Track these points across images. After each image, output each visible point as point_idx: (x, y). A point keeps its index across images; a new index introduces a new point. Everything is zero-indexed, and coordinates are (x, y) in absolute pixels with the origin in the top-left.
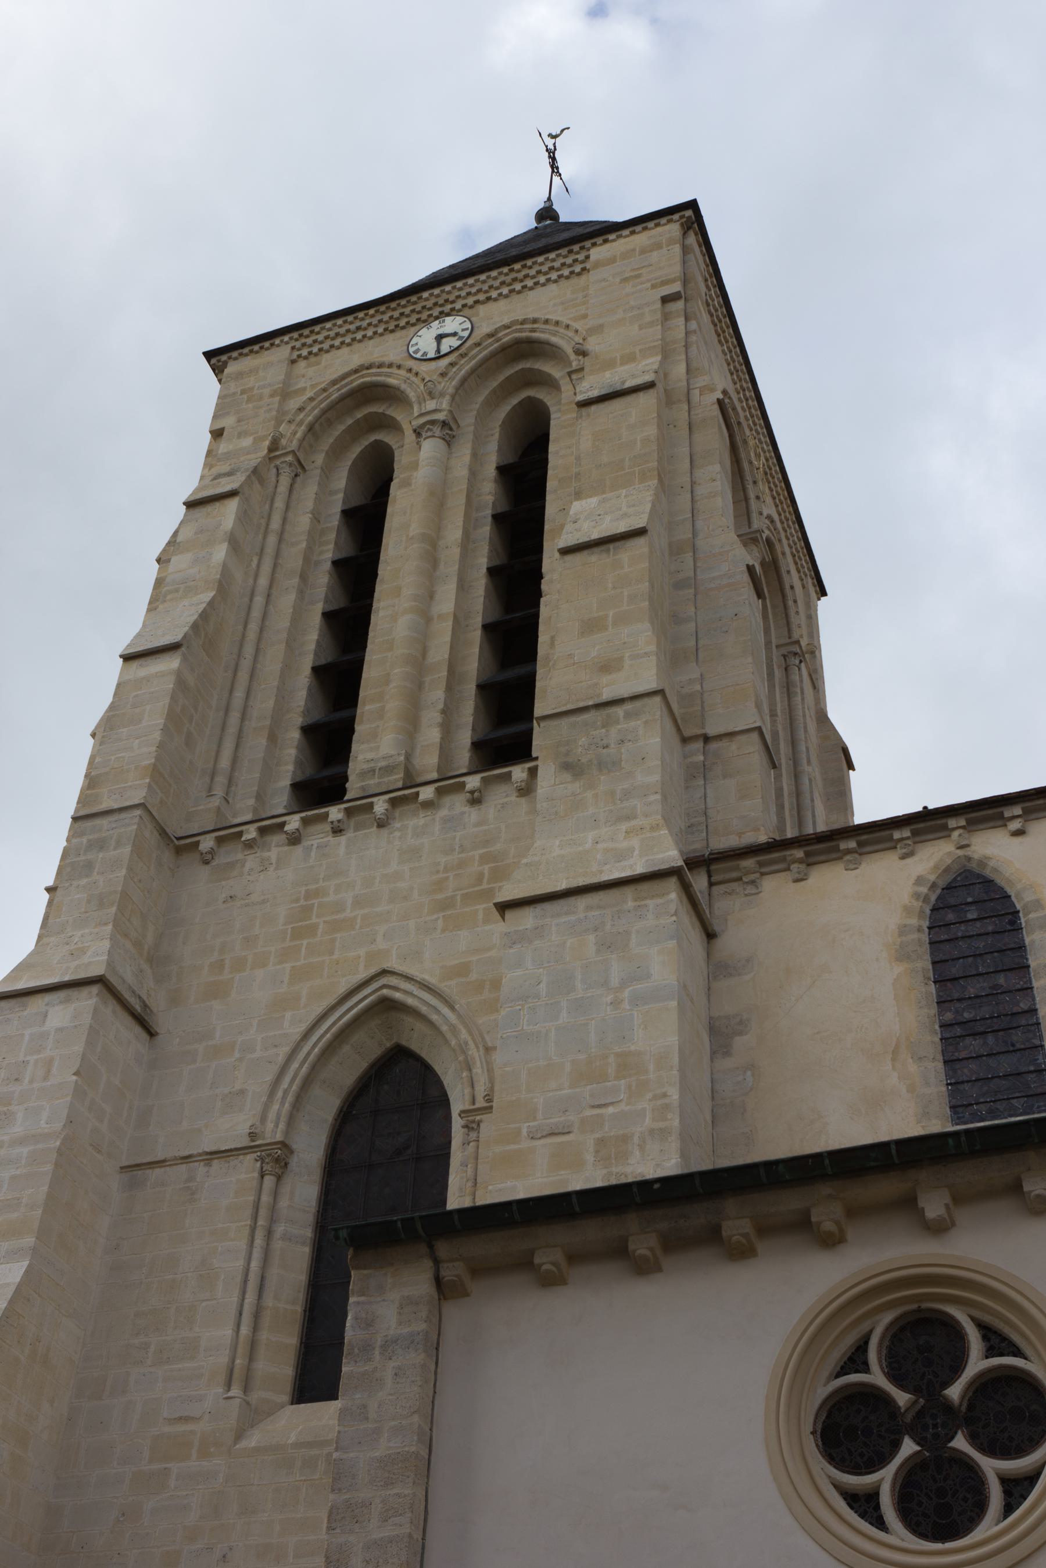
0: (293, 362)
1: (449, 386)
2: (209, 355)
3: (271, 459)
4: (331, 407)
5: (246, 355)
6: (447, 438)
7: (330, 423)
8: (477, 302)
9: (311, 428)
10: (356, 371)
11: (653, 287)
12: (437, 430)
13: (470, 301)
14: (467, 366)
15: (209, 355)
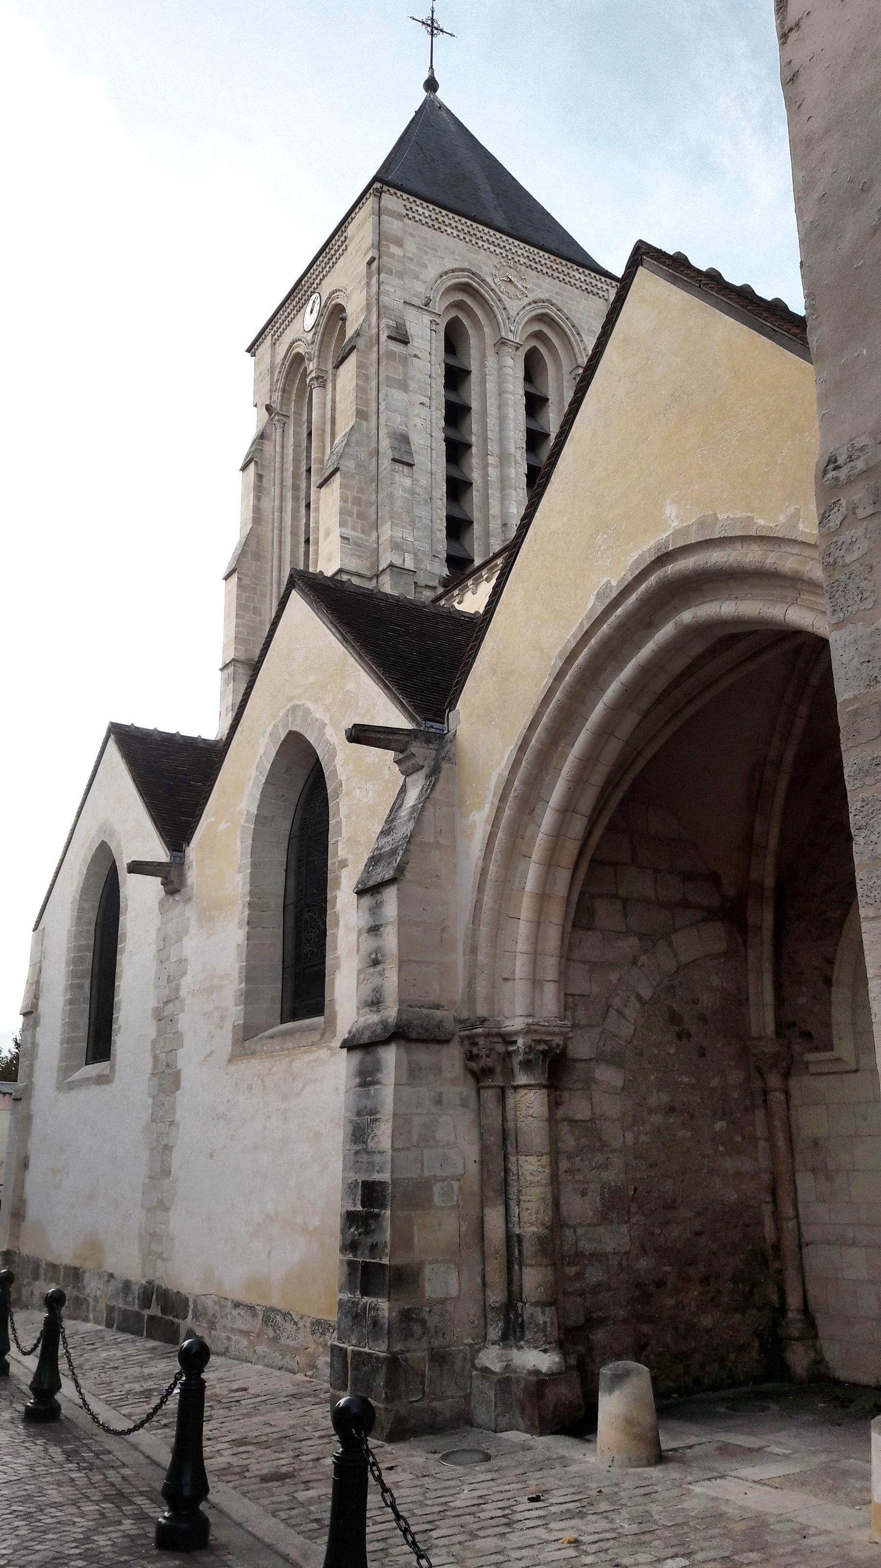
0: (275, 344)
1: (316, 347)
2: (249, 350)
3: (272, 420)
4: (288, 373)
5: (260, 345)
6: (322, 384)
7: (293, 381)
8: (321, 280)
9: (284, 391)
10: (290, 347)
11: (365, 255)
12: (315, 383)
13: (318, 281)
14: (321, 330)
15: (249, 350)
